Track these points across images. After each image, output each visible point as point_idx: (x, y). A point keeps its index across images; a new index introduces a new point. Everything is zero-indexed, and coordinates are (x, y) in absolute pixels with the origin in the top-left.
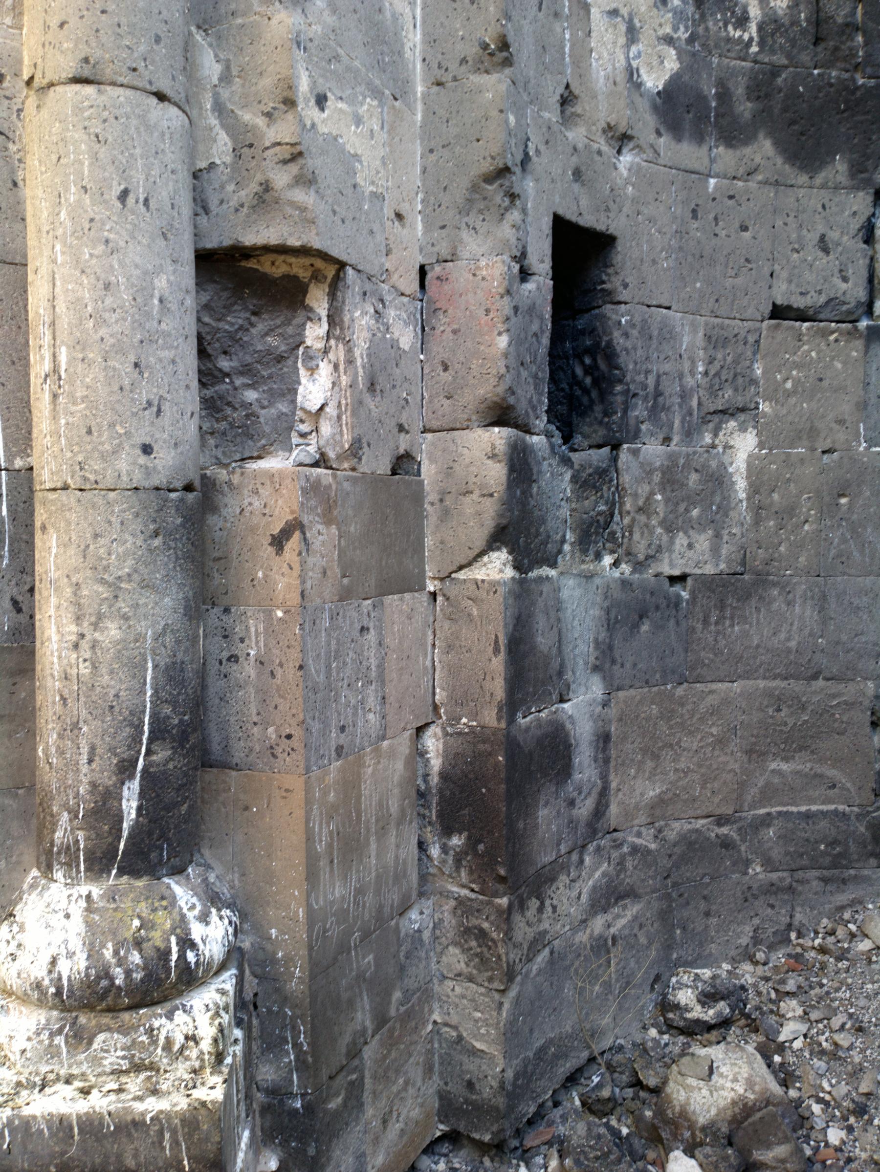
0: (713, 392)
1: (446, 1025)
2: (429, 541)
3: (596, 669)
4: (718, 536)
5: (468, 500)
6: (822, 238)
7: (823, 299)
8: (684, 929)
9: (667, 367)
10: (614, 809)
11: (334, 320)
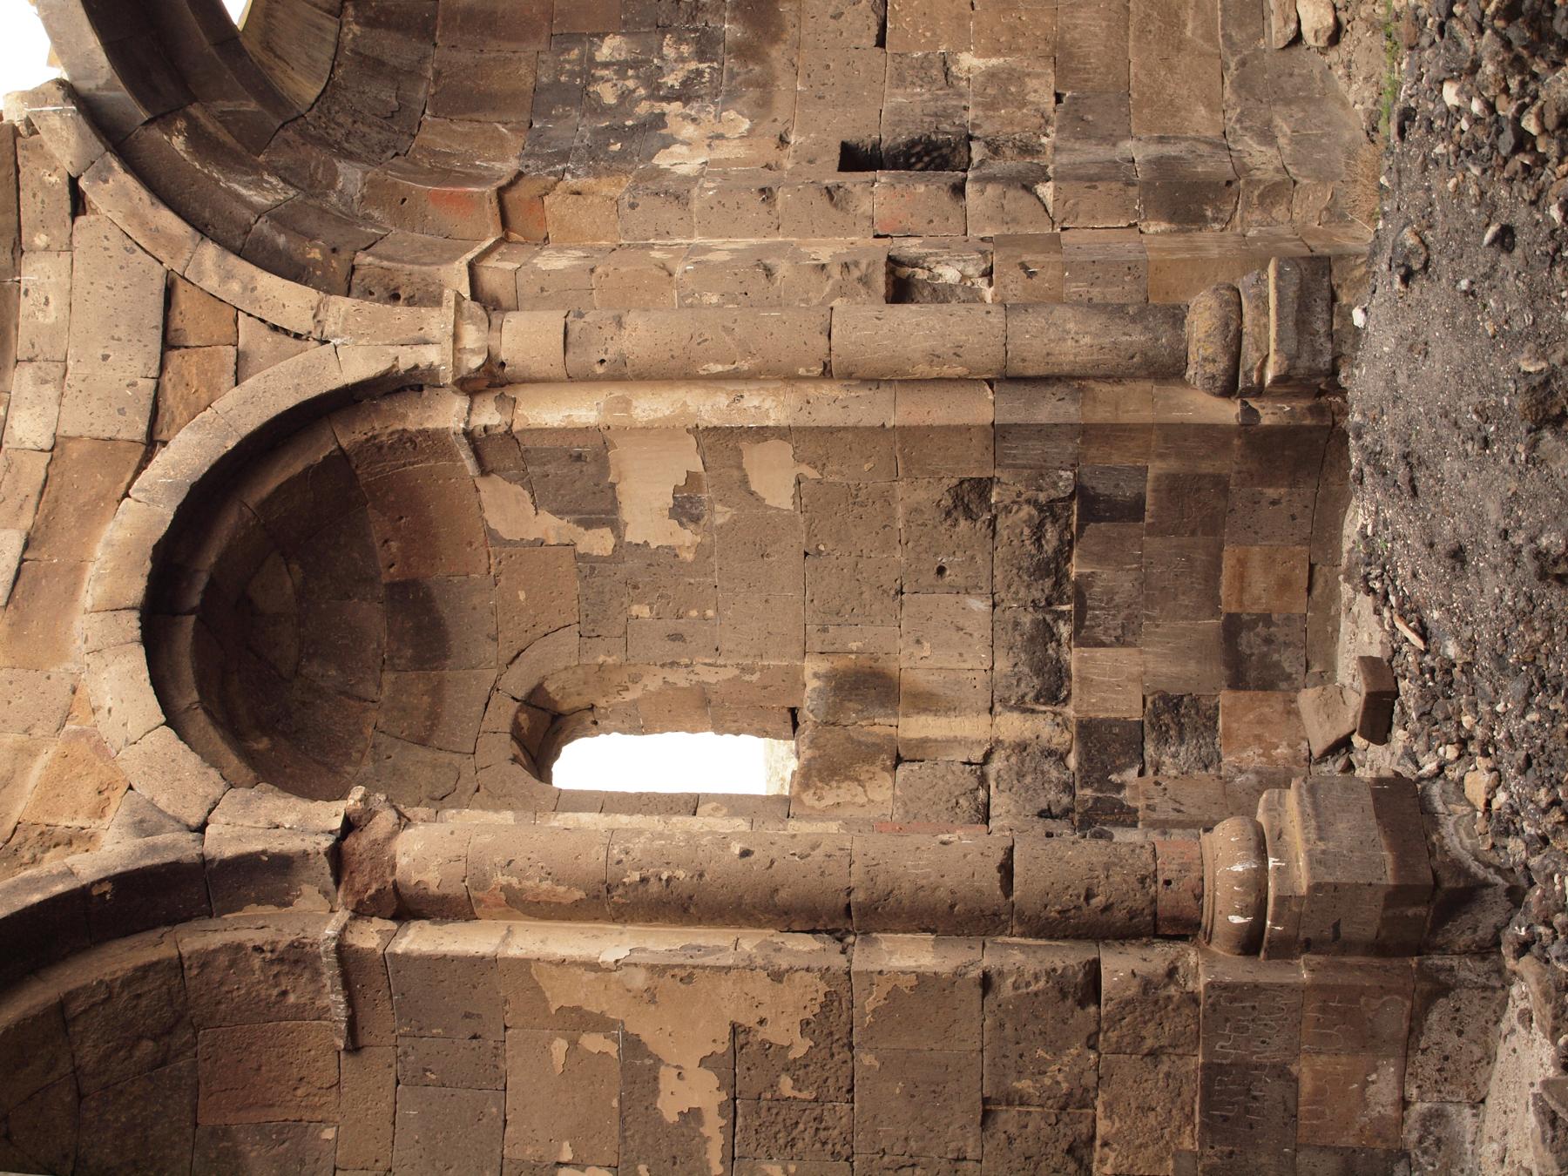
0: (933, 81)
1: (1320, 218)
2: (1031, 231)
3: (1114, 145)
4: (1028, 75)
5: (1006, 207)
6: (833, 17)
7: (872, 15)
8: (1299, 90)
9: (918, 111)
10: (1210, 134)
11: (915, 265)
